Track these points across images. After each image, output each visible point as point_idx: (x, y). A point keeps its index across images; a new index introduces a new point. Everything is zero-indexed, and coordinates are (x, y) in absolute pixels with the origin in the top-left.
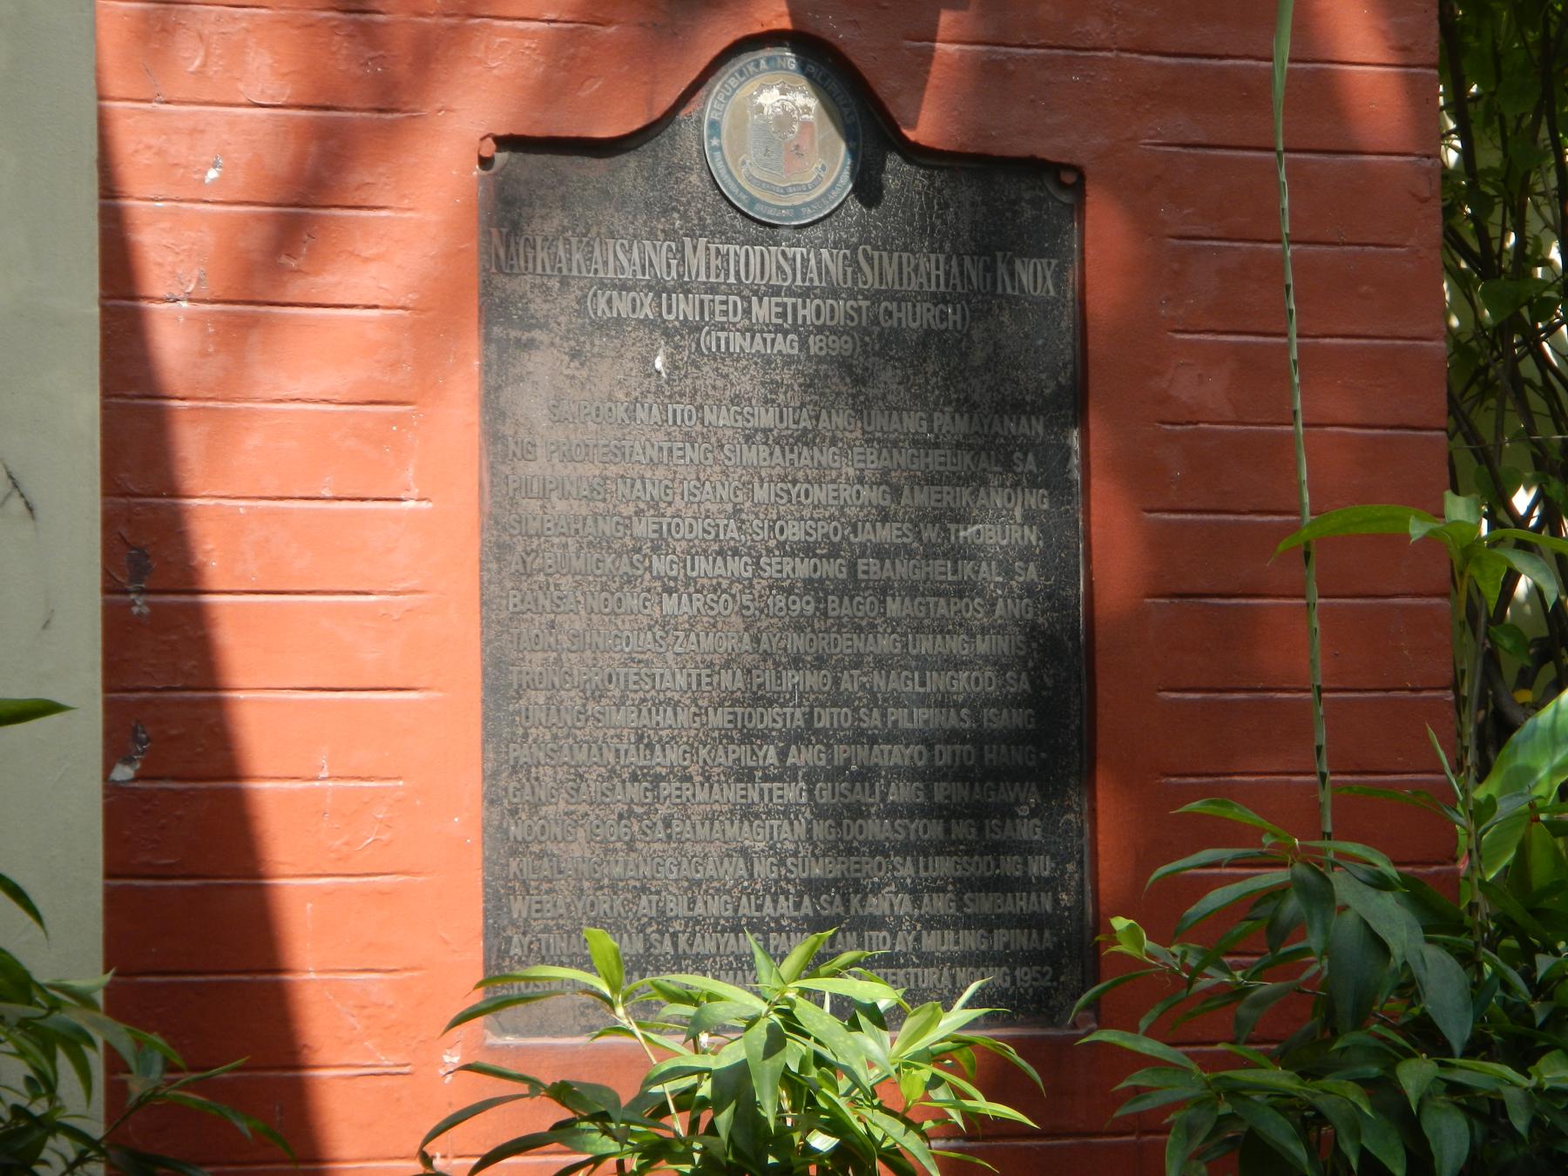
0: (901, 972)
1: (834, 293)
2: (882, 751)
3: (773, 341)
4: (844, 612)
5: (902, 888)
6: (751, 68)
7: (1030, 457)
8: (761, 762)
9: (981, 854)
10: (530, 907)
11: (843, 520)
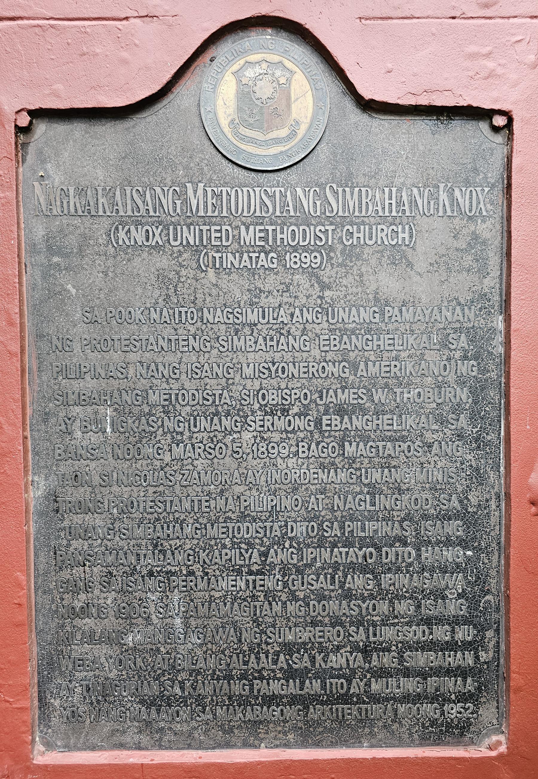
0: (355, 708)
2: (341, 553)
5: (355, 648)
8: (247, 562)
9: (418, 625)
10: (74, 663)
11: (311, 388)
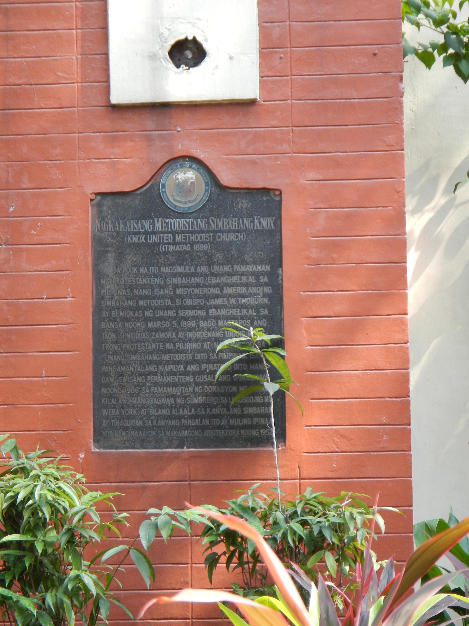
1: (202, 232)
3: (182, 247)
4: (205, 325)
5: (223, 406)
6: (175, 168)
7: (266, 277)
